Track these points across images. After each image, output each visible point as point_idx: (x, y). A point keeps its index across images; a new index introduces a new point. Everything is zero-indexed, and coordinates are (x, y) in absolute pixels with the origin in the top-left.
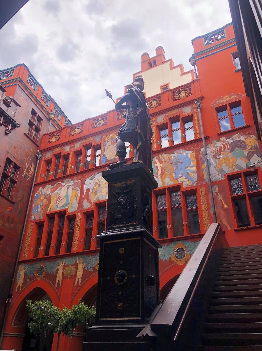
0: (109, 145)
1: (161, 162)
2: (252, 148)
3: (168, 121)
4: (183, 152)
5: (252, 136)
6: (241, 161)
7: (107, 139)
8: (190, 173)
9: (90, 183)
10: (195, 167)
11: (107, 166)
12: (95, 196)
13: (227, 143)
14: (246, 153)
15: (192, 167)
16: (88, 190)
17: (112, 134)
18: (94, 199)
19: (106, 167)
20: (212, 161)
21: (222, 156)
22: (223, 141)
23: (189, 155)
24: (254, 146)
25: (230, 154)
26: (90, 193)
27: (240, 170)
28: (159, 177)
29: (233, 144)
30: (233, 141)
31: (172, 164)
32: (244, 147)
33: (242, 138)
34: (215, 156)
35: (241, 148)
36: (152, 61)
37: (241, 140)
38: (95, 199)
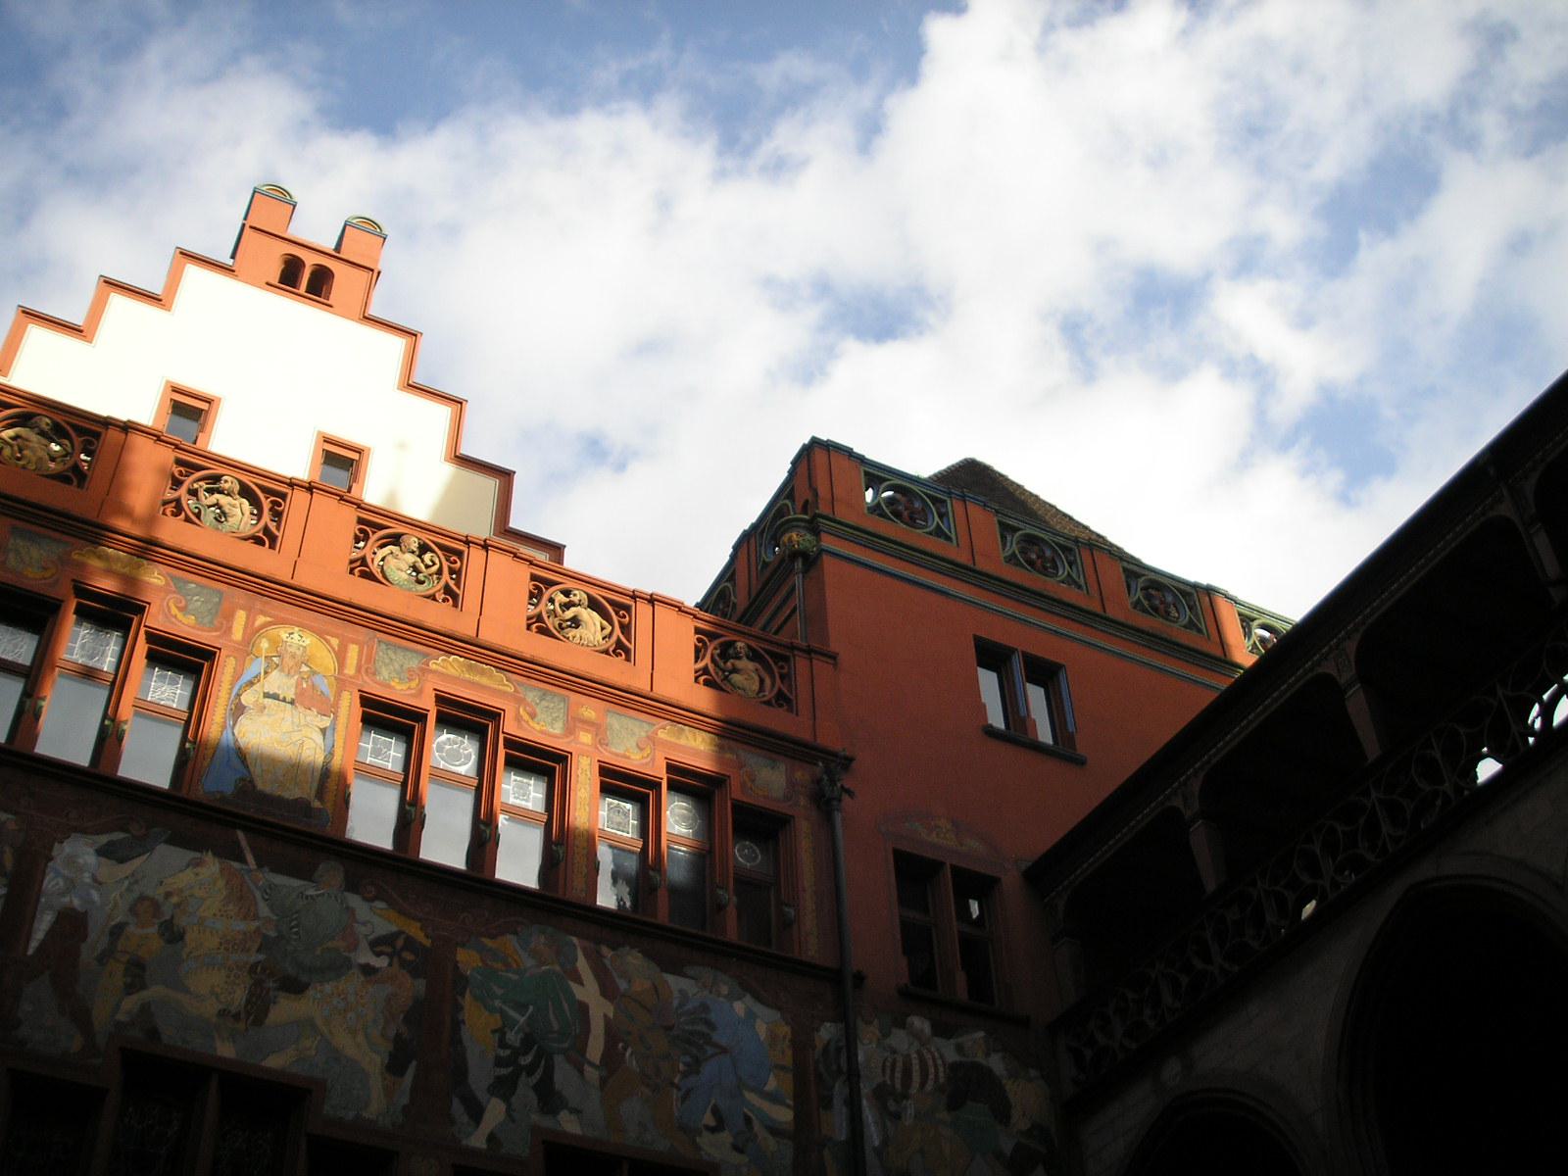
0: (275, 697)
1: (608, 990)
3: (661, 772)
4: (732, 997)
5: (1033, 1073)
7: (265, 644)
8: (757, 1126)
9: (95, 879)
10: (788, 1106)
11: (245, 829)
12: (130, 989)
14: (1007, 1146)
15: (774, 1098)
16: (72, 924)
17: (309, 640)
18: (113, 1006)
19: (241, 835)
20: (869, 1114)
21: (910, 1109)
23: (762, 1029)
25: (944, 1115)
26: (84, 948)
28: (592, 1074)
31: (669, 1028)
32: (1002, 1112)
33: (996, 1064)
34: (881, 1094)
36: (310, 260)
37: (990, 1071)
38: (121, 1017)
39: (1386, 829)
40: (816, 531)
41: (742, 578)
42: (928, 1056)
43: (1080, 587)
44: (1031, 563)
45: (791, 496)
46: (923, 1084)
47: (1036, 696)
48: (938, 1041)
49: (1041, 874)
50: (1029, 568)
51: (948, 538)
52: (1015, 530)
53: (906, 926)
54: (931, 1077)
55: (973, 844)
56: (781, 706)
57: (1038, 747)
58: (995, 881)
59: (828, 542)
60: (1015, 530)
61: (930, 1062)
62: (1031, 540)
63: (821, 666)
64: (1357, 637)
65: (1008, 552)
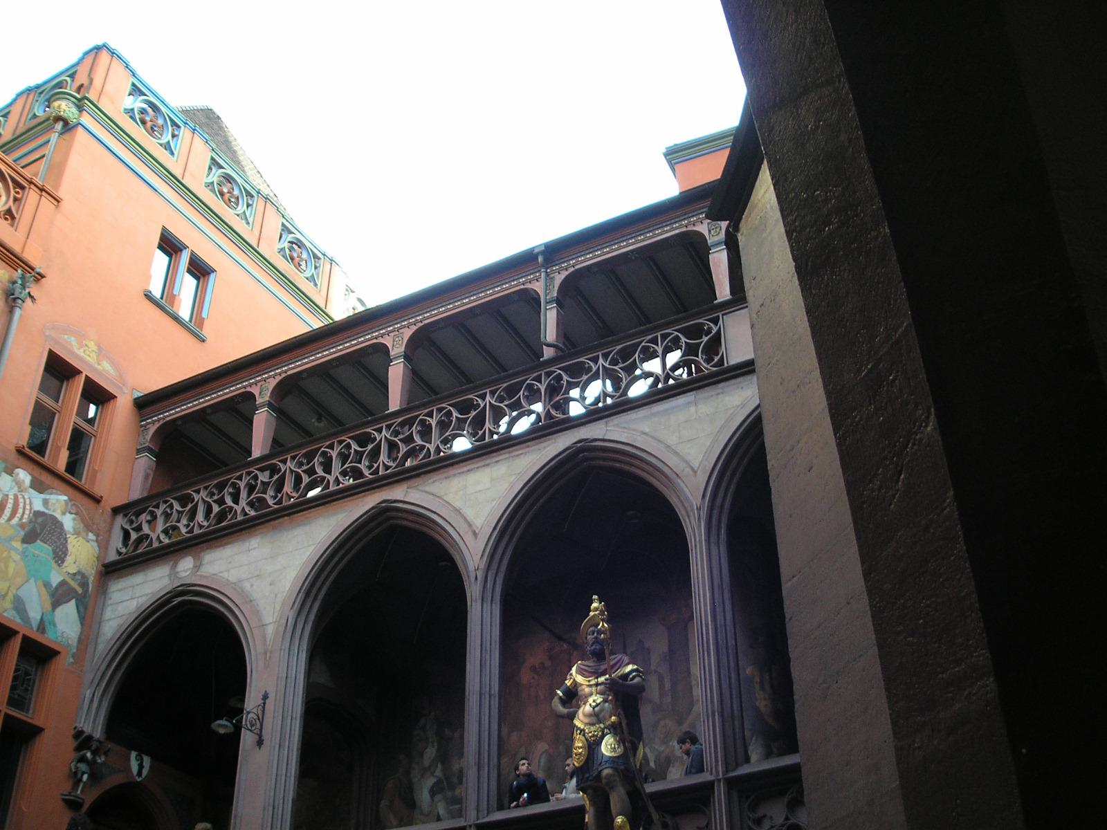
2: (75, 574)
5: (91, 536)
6: (34, 590)
13: (28, 502)
14: (55, 579)
22: (19, 484)
24: (83, 576)
25: (17, 544)
27: (18, 620)
29: (40, 520)
30: (42, 509)
32: (60, 556)
33: (68, 522)
35: (54, 552)
37: (61, 525)
39: (383, 457)
40: (80, 108)
41: (13, 118)
42: (21, 500)
43: (248, 223)
44: (222, 194)
45: (72, 76)
46: (10, 519)
47: (188, 284)
48: (30, 490)
49: (145, 404)
50: (290, 261)
51: (172, 154)
52: (221, 167)
53: (39, 407)
54: (18, 515)
55: (106, 366)
56: (6, 219)
57: (176, 319)
58: (114, 397)
59: (86, 120)
60: (221, 167)
61: (21, 505)
62: (228, 179)
63: (46, 203)
64: (414, 328)
65: (209, 180)
